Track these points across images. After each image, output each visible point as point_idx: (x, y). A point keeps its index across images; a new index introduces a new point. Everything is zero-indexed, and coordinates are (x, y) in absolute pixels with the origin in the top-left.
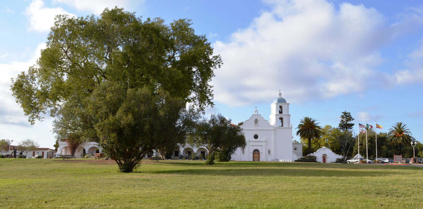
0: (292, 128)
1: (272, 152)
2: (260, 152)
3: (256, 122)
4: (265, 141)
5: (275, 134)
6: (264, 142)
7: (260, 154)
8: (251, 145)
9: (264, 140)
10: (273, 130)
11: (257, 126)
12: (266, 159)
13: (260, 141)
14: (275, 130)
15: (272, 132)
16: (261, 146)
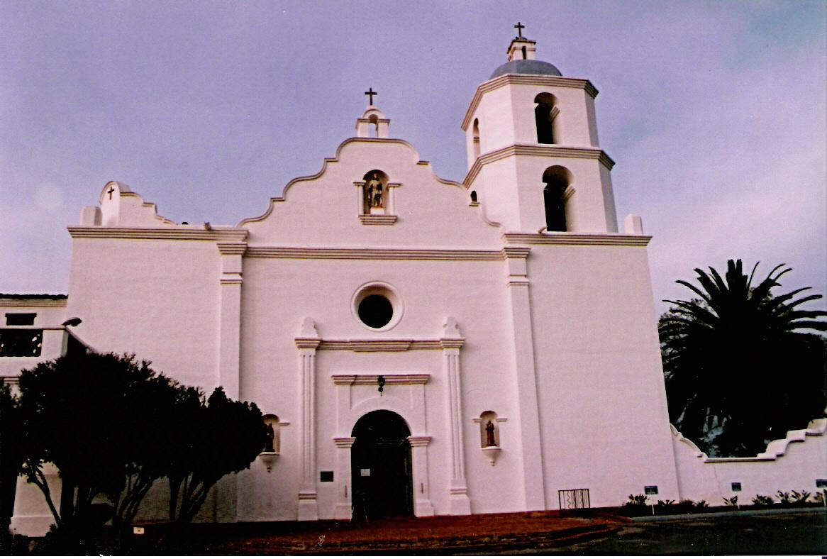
0: (649, 238)
1: (512, 435)
2: (416, 432)
3: (375, 192)
4: (449, 344)
5: (529, 286)
6: (445, 351)
7: (417, 453)
8: (340, 380)
9: (440, 335)
10: (512, 253)
11: (381, 220)
12: (468, 493)
13: (411, 345)
14: (528, 256)
15: (505, 267)
16: (426, 380)
